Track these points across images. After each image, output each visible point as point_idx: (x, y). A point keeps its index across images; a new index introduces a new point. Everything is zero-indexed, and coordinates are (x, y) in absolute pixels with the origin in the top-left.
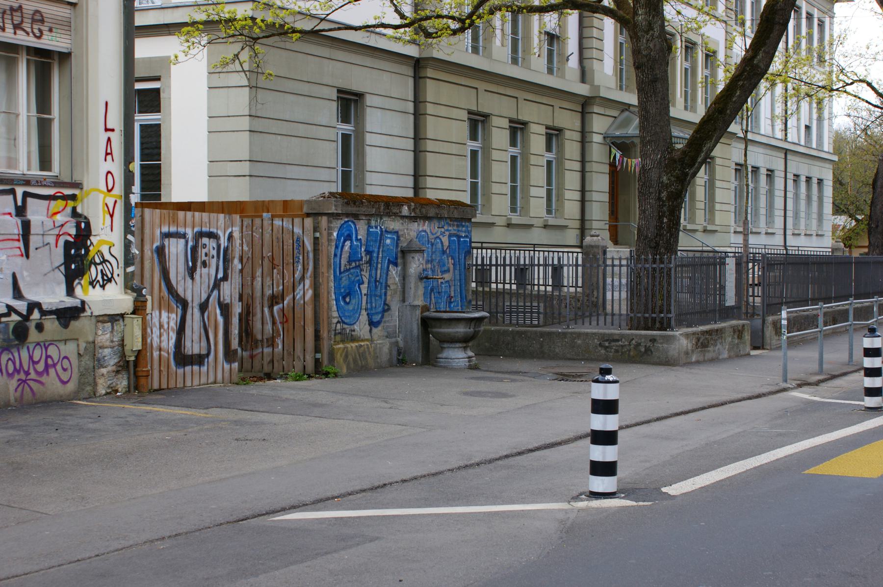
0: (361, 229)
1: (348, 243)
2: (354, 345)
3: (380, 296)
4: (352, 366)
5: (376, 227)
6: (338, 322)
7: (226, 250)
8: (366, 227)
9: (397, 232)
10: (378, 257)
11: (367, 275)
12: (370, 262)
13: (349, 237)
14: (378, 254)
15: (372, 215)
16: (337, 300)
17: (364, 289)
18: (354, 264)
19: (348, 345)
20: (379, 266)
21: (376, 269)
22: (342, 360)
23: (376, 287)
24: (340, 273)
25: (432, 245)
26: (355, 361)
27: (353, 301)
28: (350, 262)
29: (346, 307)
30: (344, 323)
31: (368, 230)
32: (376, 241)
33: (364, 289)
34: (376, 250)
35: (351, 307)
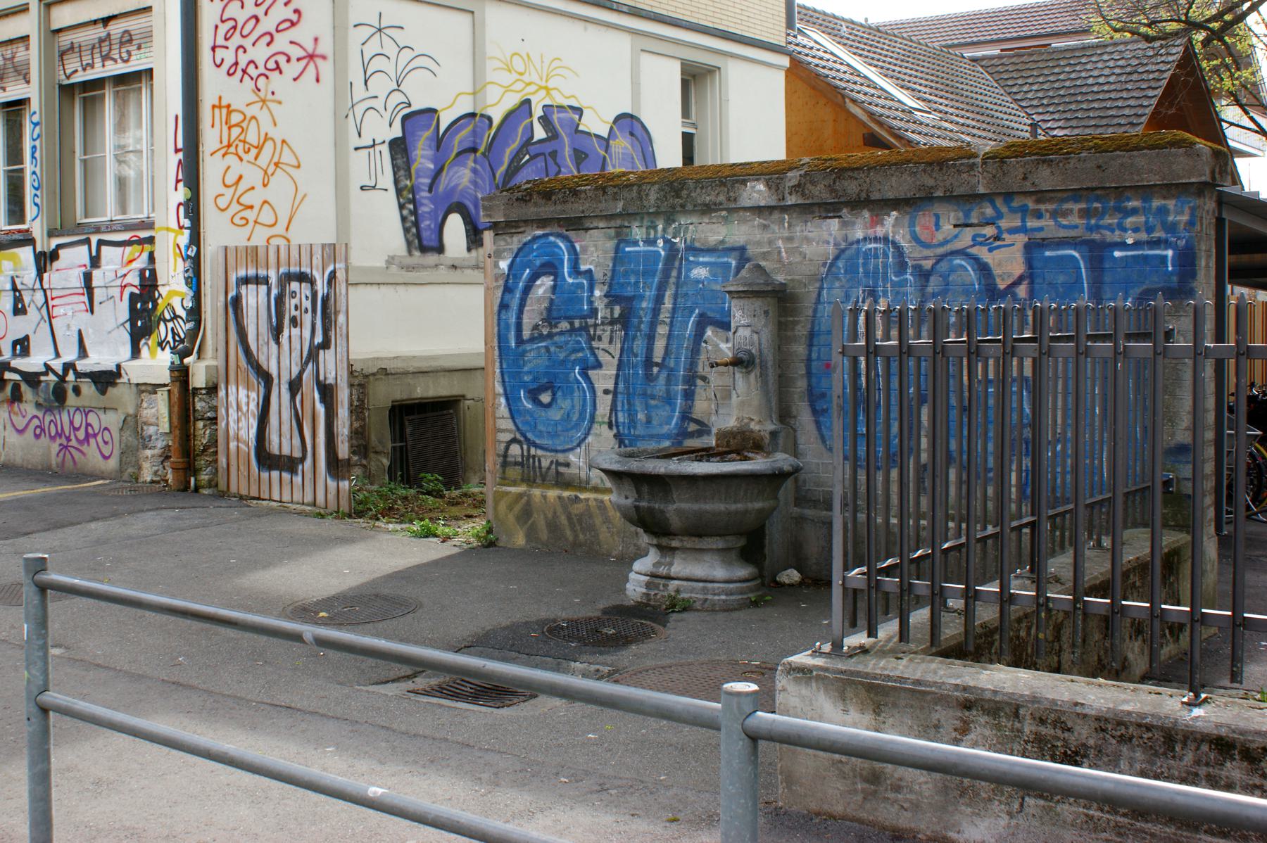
0: (595, 251)
1: (545, 283)
2: (553, 494)
3: (669, 399)
4: (544, 535)
5: (651, 242)
6: (514, 440)
7: (325, 300)
8: (611, 244)
9: (742, 249)
10: (656, 312)
11: (616, 348)
12: (625, 321)
13: (551, 268)
14: (659, 300)
15: (627, 215)
16: (511, 400)
17: (604, 379)
18: (564, 325)
19: (537, 492)
20: (662, 330)
21: (651, 338)
22: (511, 518)
23: (649, 378)
24: (520, 341)
25: (924, 275)
26: (553, 526)
27: (565, 404)
28: (550, 317)
29: (542, 413)
30: (531, 443)
31: (617, 249)
32: (649, 273)
33: (604, 379)
34: (650, 293)
35: (555, 415)
